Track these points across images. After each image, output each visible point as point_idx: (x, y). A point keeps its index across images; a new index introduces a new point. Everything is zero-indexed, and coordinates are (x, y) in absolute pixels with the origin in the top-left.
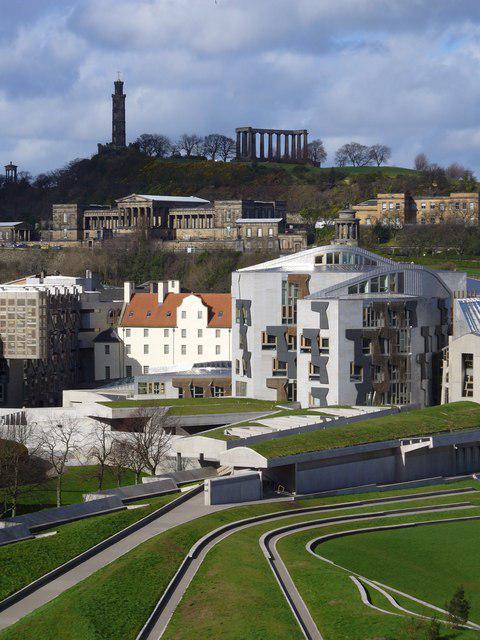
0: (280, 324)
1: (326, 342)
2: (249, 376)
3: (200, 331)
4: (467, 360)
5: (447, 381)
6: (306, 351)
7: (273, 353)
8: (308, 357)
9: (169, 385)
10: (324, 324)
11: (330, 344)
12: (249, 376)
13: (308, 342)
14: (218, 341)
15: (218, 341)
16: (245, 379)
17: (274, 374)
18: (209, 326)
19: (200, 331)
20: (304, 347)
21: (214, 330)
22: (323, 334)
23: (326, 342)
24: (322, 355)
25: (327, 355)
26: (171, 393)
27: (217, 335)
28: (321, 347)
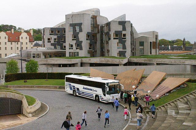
0: (90, 32)
1: (125, 35)
2: (81, 49)
3: (6, 43)
4: (142, 44)
5: (133, 50)
6: (114, 39)
7: (89, 41)
8: (117, 41)
9: (42, 55)
10: (124, 29)
11: (126, 36)
12: (81, 49)
13: (117, 35)
14: (12, 46)
15: (12, 46)
16: (78, 50)
17: (89, 48)
18: (9, 41)
19: (6, 43)
20: (115, 37)
21: (10, 42)
22: (124, 32)
23: (125, 35)
24: (123, 40)
25: (125, 40)
26: (43, 57)
27: (11, 44)
28: (123, 37)
